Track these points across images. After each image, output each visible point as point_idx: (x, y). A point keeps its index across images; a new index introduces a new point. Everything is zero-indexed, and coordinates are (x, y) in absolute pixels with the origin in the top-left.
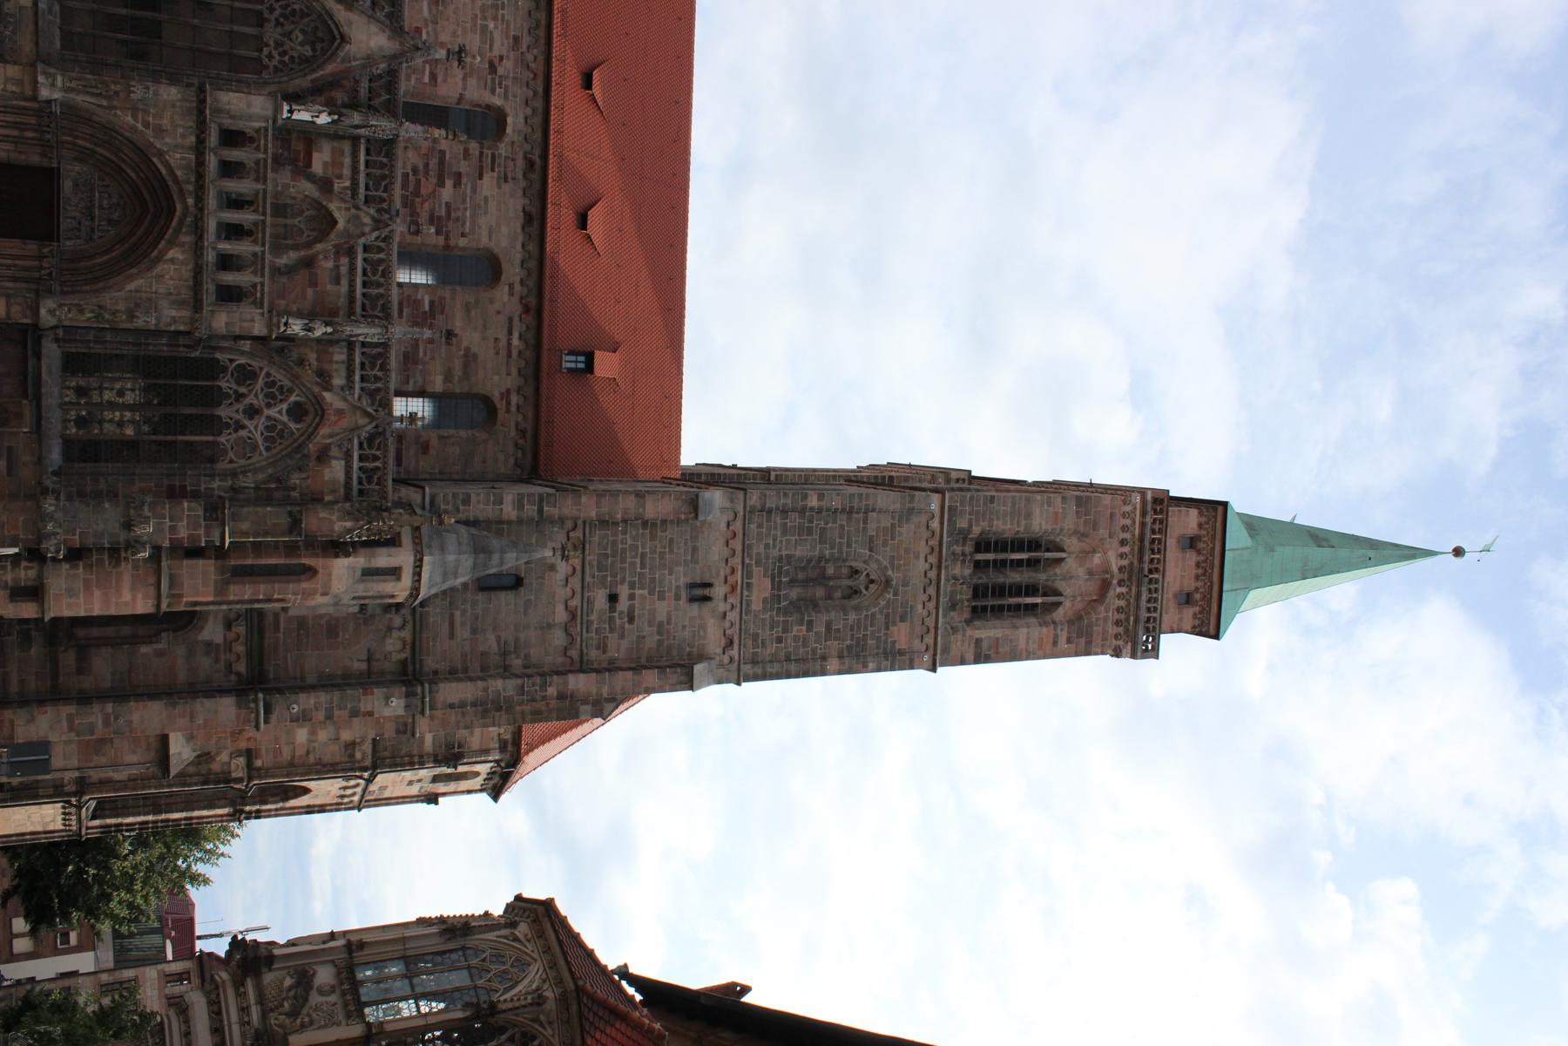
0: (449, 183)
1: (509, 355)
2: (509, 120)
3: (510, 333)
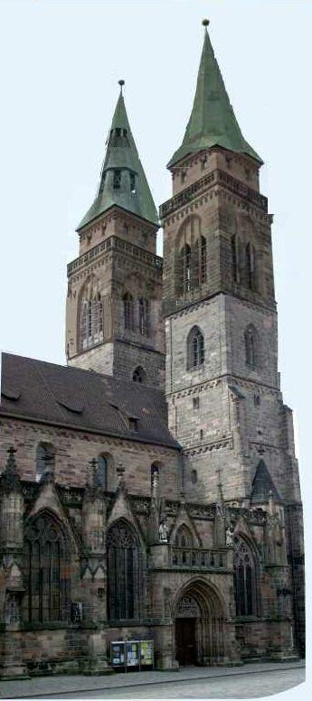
0: (73, 470)
1: (136, 453)
2: (44, 440)
3: (128, 452)
